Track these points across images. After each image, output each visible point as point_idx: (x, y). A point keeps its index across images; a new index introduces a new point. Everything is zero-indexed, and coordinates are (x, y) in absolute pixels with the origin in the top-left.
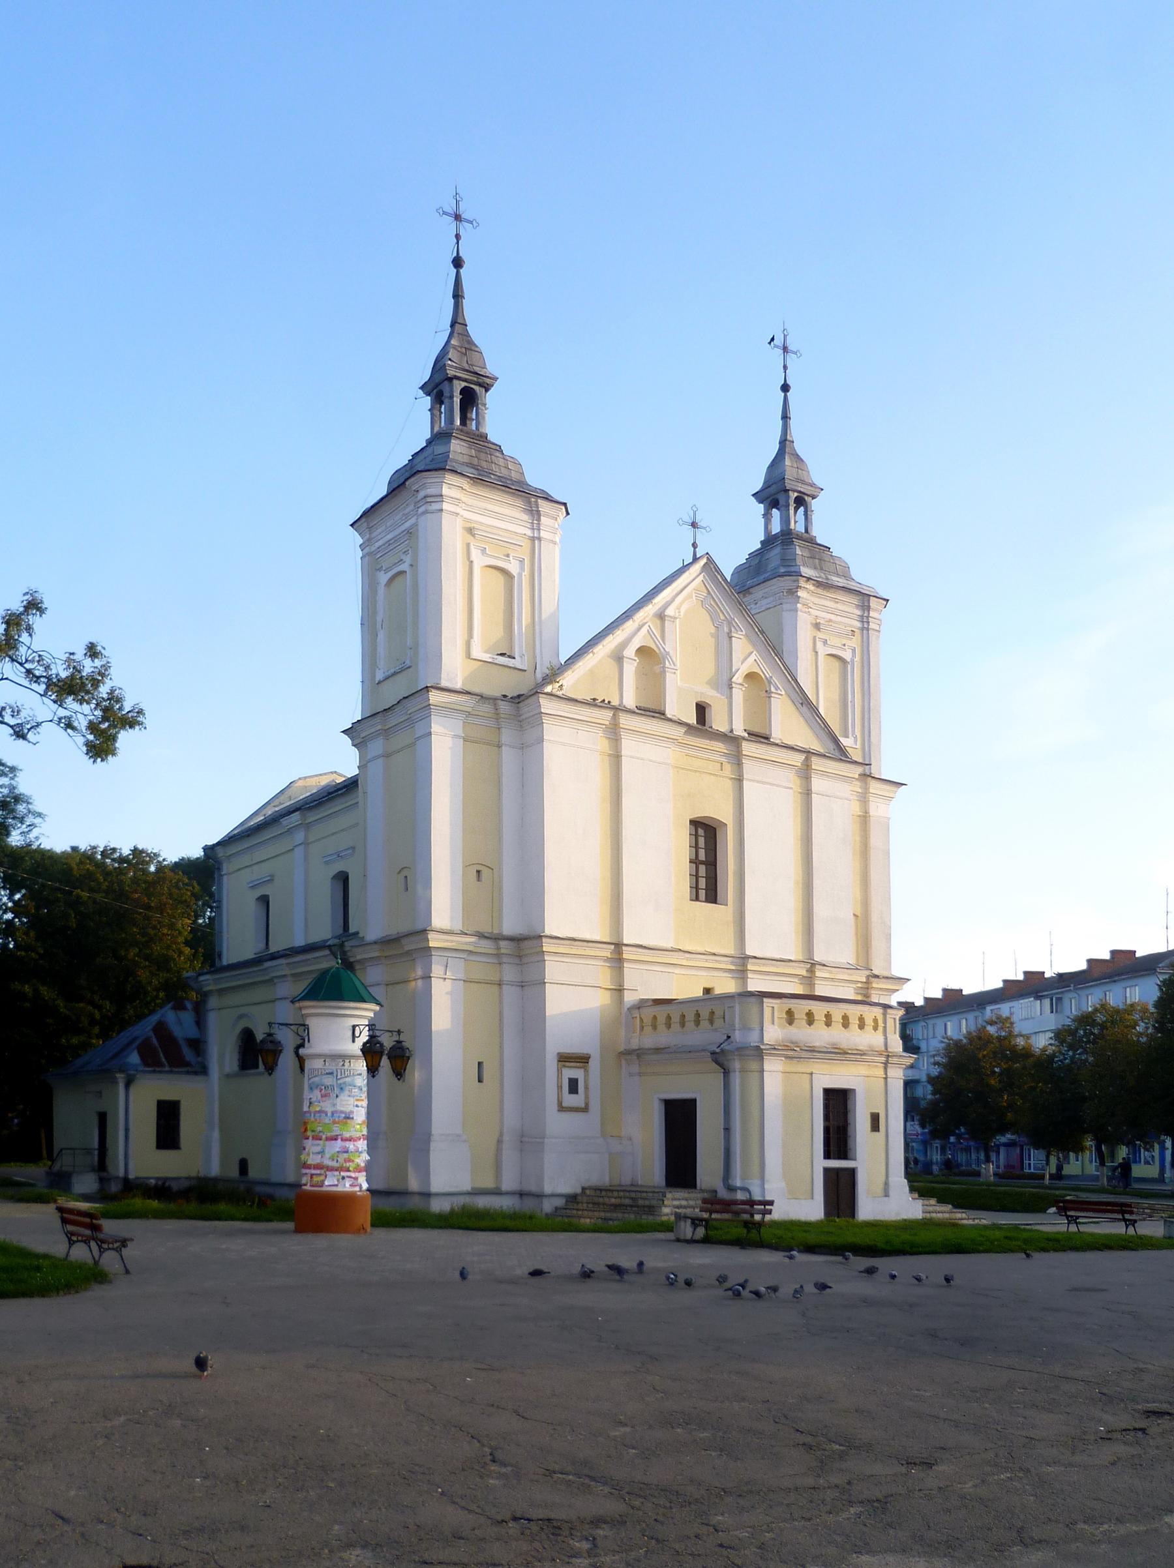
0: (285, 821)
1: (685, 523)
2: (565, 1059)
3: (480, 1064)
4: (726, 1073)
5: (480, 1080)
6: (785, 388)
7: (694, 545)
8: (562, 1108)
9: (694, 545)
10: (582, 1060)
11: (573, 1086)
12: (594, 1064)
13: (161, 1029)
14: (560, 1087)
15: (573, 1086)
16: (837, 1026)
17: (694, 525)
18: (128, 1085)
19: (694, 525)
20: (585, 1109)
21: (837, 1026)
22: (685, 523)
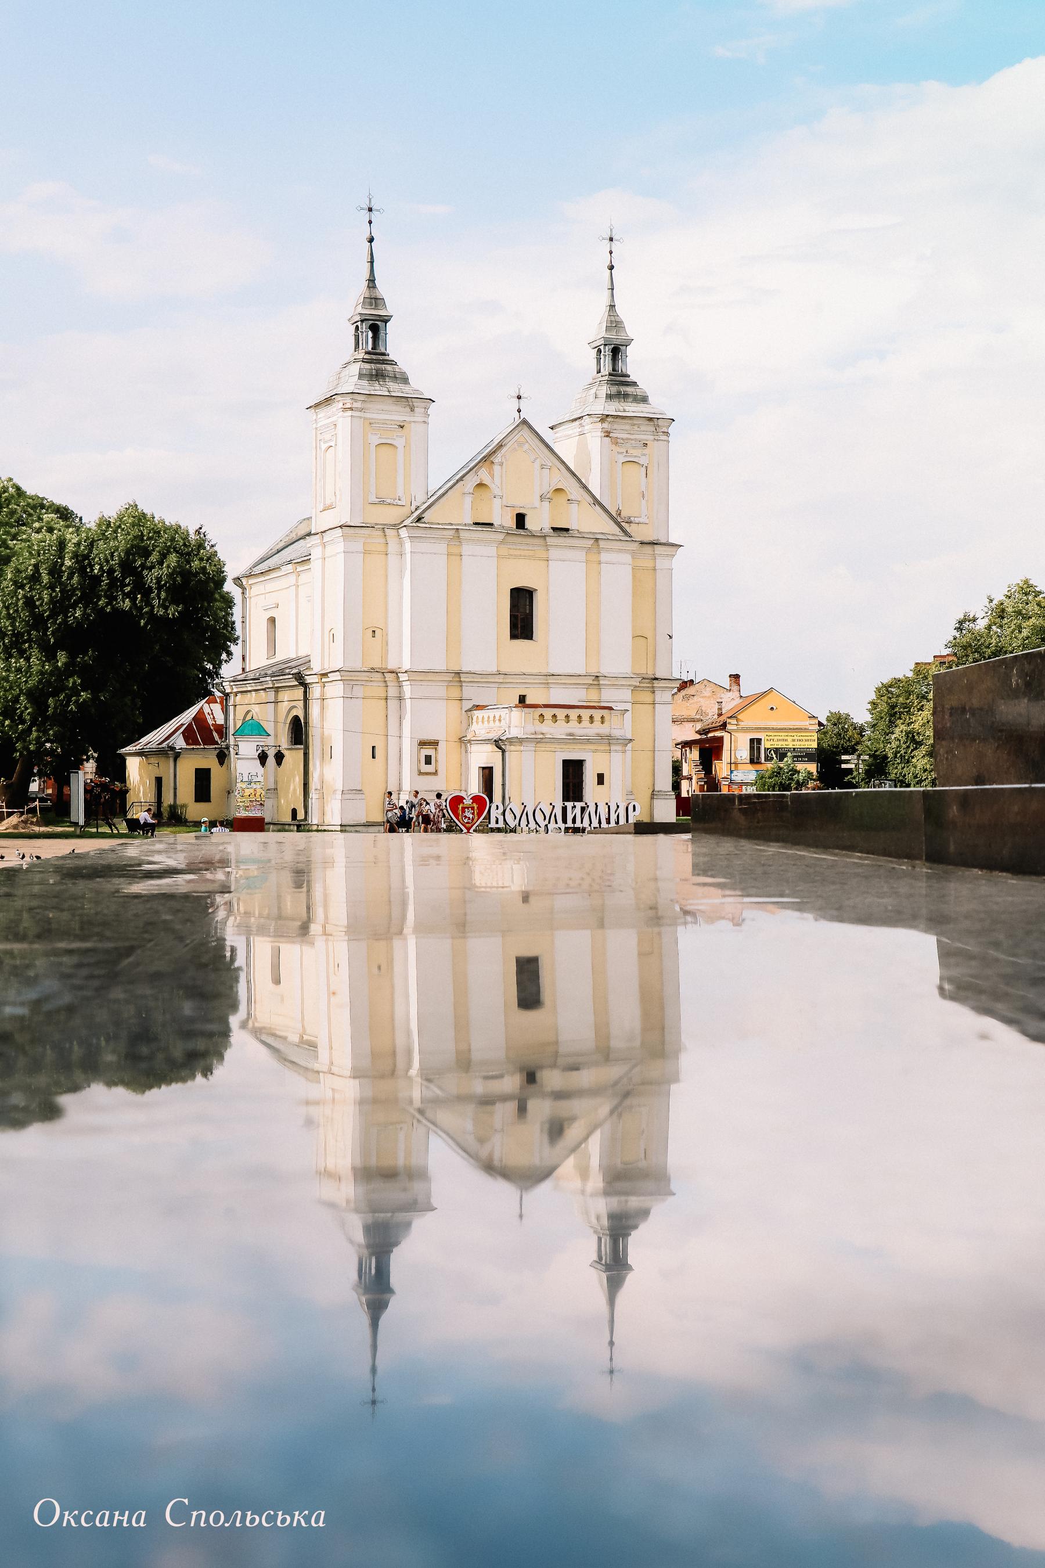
0: (283, 568)
1: (512, 397)
2: (423, 744)
3: (373, 747)
4: (503, 751)
5: (374, 757)
6: (611, 268)
7: (519, 411)
8: (420, 773)
9: (519, 411)
10: (434, 744)
11: (428, 760)
12: (442, 746)
13: (199, 719)
14: (419, 761)
15: (428, 760)
16: (573, 723)
17: (519, 397)
18: (175, 761)
19: (519, 397)
20: (436, 773)
21: (573, 723)
22: (512, 397)
